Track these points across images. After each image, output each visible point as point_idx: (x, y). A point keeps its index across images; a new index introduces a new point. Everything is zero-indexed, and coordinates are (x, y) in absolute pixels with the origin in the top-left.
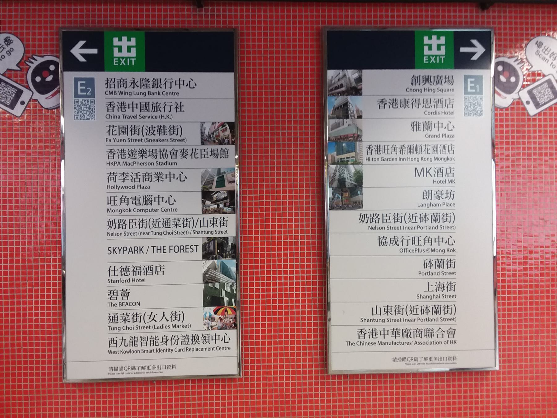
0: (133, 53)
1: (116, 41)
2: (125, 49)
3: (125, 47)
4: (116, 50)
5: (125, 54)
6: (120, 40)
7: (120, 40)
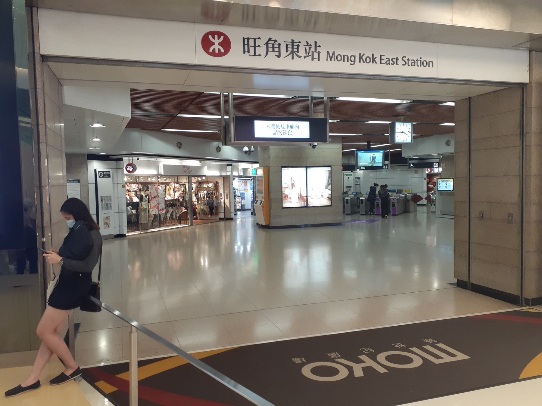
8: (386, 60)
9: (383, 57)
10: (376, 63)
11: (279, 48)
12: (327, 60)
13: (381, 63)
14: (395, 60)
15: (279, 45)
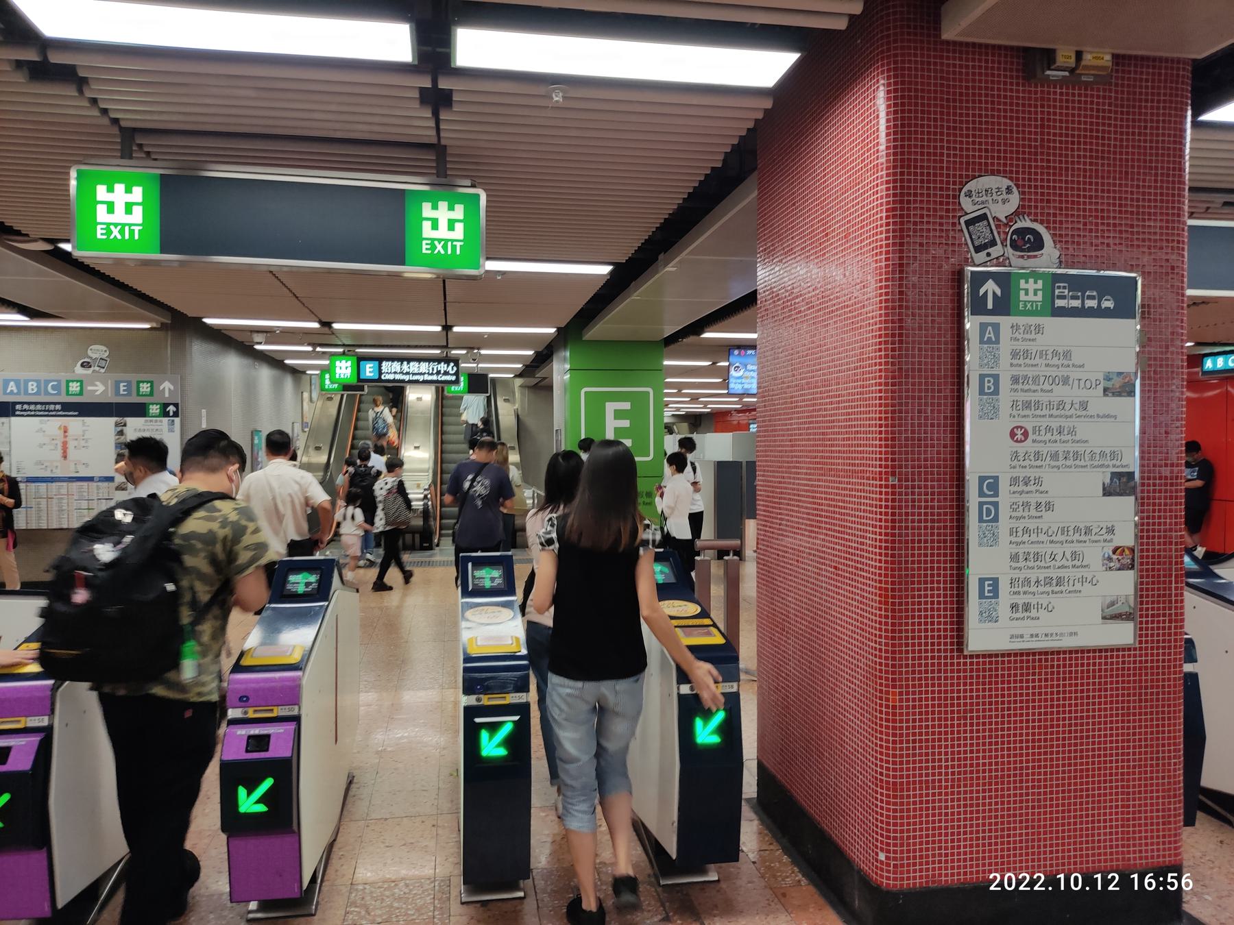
0: (1039, 297)
2: (1031, 292)
4: (1022, 293)
5: (1031, 297)
6: (1027, 282)
7: (1027, 282)
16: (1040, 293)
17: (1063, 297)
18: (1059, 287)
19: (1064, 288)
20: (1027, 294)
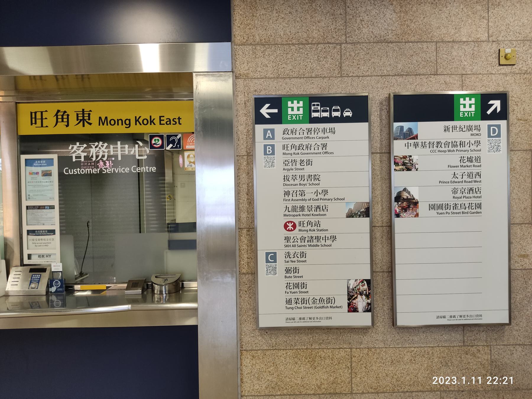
0: (301, 111)
1: (290, 104)
3: (295, 108)
4: (290, 110)
6: (292, 103)
7: (292, 103)
8: (166, 121)
9: (162, 118)
10: (154, 124)
11: (68, 118)
12: (99, 125)
13: (160, 124)
14: (177, 121)
15: (68, 115)
16: (301, 109)
17: (317, 111)
18: (314, 105)
19: (318, 105)
20: (293, 110)
